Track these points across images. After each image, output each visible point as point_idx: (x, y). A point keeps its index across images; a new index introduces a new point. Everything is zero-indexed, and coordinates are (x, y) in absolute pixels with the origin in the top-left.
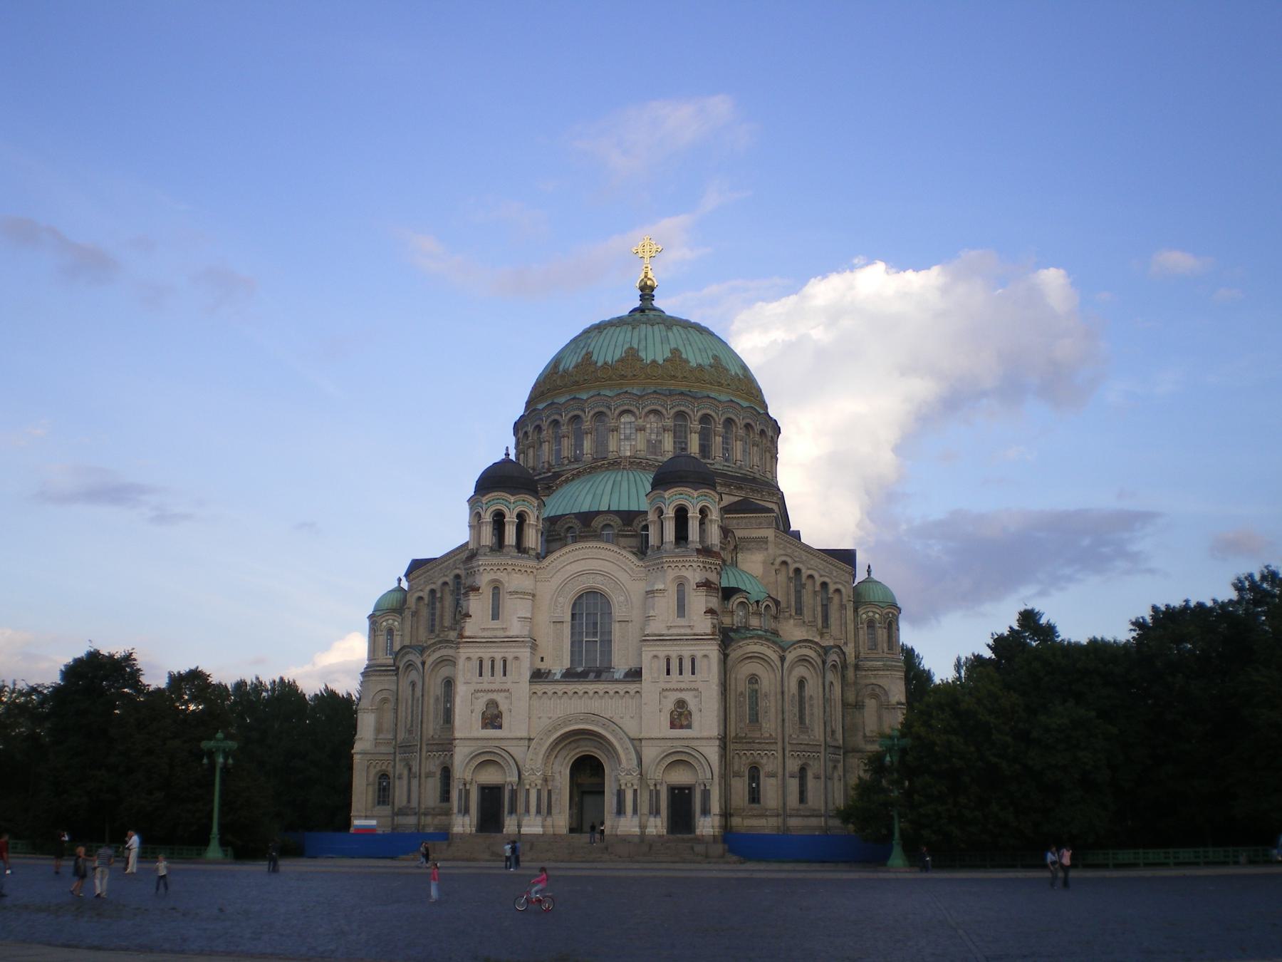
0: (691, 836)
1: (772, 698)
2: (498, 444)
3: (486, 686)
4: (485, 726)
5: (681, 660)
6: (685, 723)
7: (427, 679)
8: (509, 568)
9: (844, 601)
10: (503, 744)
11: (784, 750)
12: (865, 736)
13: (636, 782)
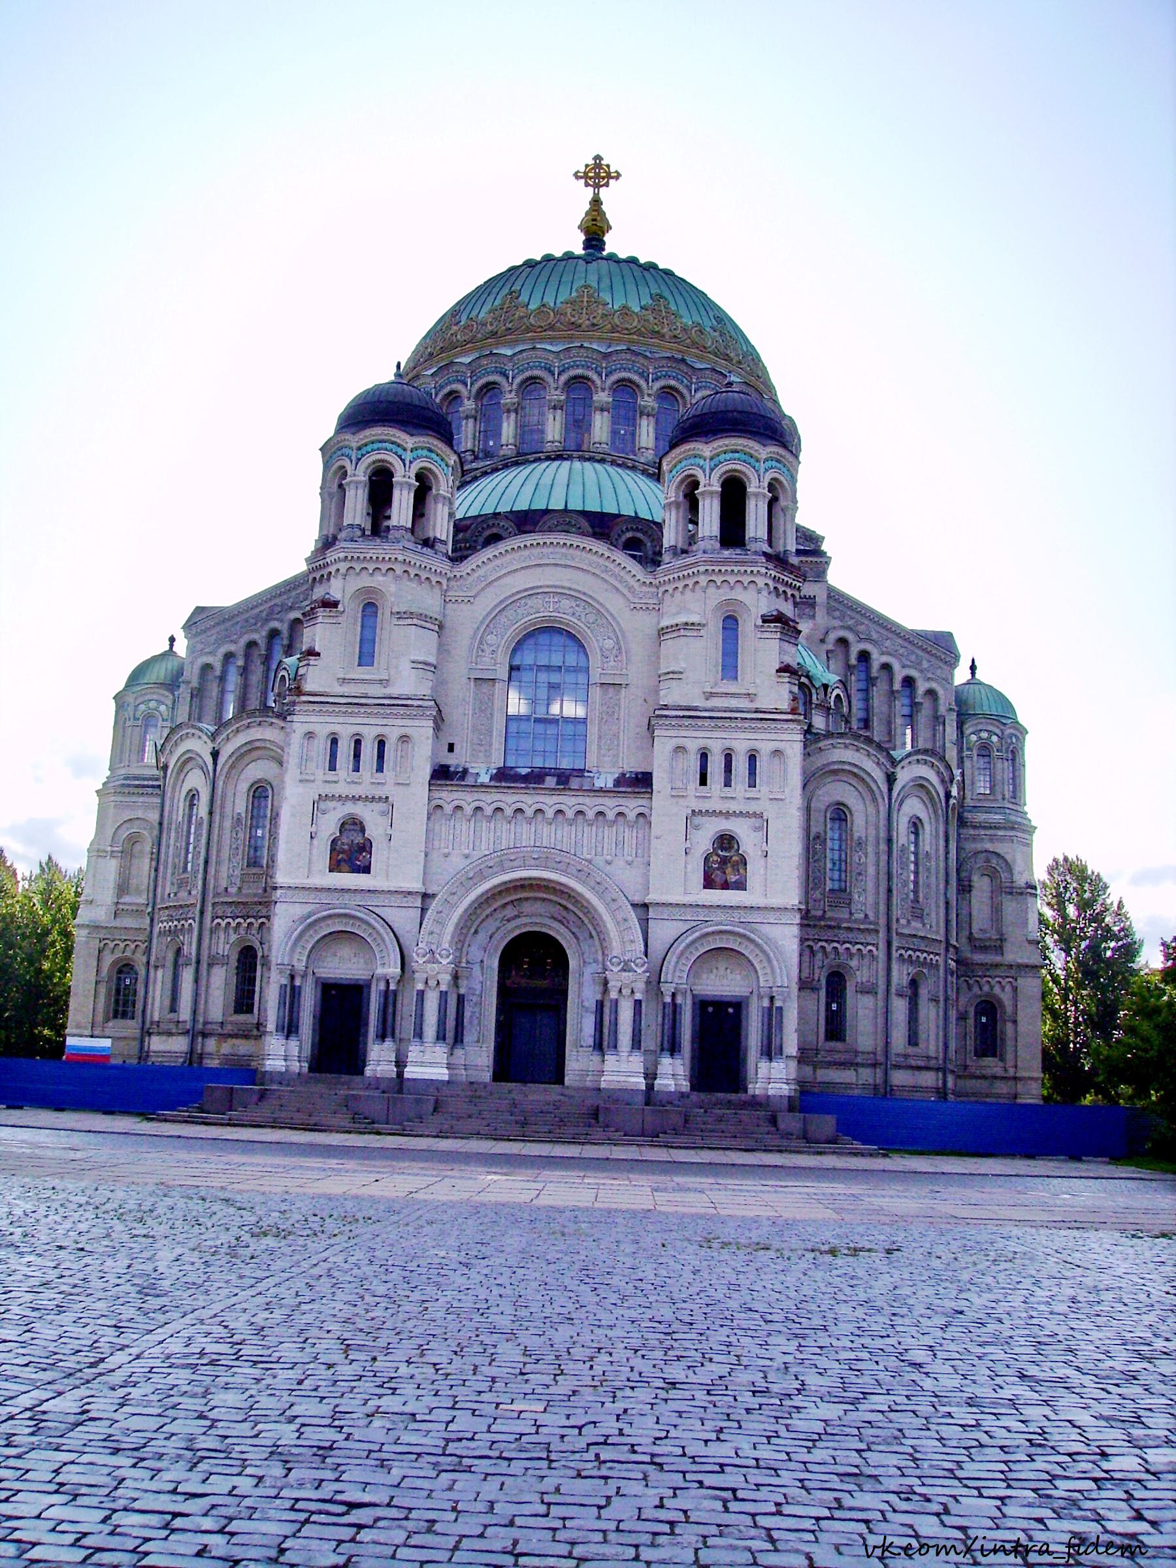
0: (742, 1096)
1: (870, 849)
2: (378, 370)
3: (342, 789)
4: (335, 867)
5: (728, 759)
6: (733, 878)
7: (220, 783)
8: (399, 569)
9: (942, 710)
10: (371, 901)
11: (889, 944)
12: (970, 938)
13: (640, 986)
